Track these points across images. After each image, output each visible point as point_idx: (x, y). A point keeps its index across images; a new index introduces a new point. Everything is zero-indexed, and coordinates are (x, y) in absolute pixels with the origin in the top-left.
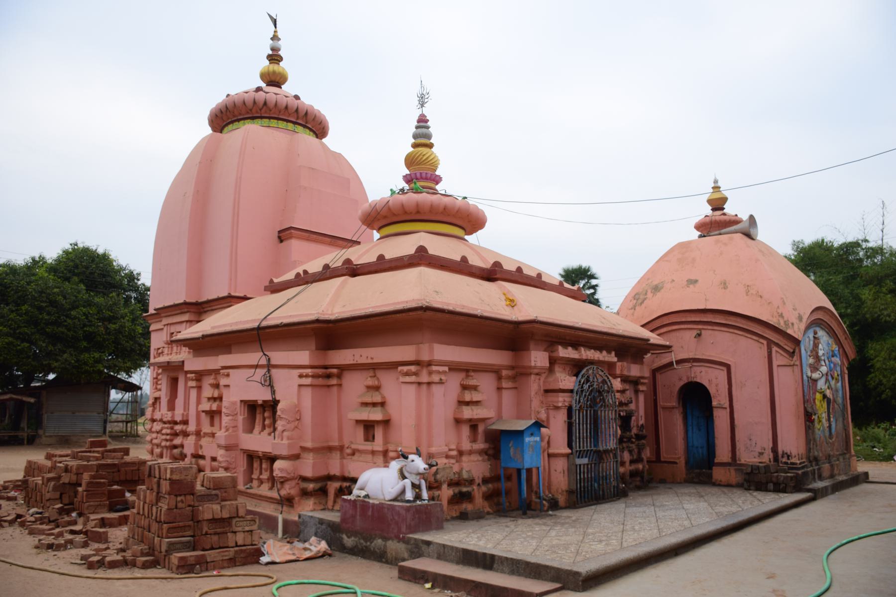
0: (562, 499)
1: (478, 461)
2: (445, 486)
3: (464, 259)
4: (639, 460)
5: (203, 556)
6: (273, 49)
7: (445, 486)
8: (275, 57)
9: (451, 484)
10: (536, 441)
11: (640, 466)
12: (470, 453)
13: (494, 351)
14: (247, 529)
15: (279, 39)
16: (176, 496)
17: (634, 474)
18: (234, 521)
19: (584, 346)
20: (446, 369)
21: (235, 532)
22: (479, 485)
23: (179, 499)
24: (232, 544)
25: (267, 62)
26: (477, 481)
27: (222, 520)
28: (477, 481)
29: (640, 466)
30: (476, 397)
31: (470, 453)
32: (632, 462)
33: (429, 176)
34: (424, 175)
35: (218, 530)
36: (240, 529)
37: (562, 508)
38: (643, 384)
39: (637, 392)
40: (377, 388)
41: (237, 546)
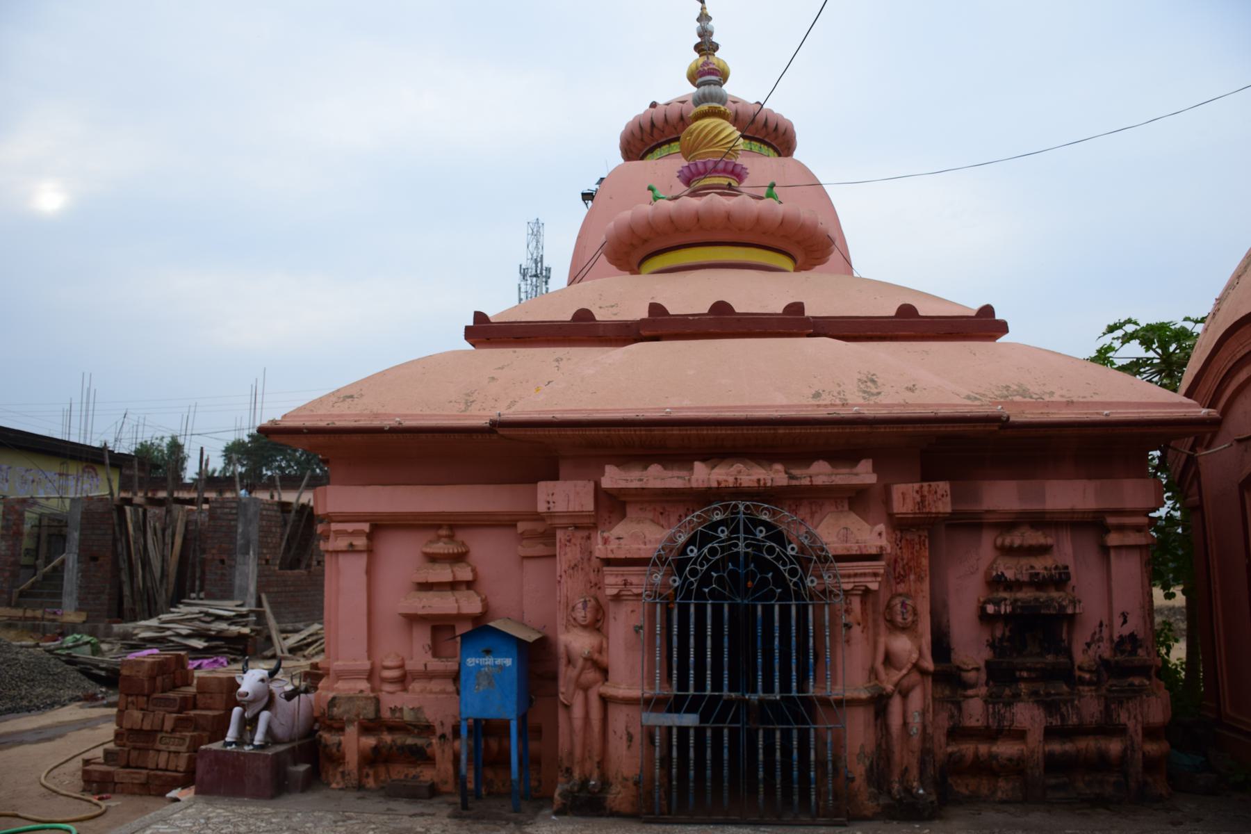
0: (618, 796)
1: (443, 692)
2: (352, 730)
3: (656, 309)
4: (1107, 728)
5: (109, 773)
6: (700, 35)
7: (352, 730)
8: (706, 46)
9: (367, 728)
10: (502, 667)
11: (1115, 747)
12: (428, 675)
13: (492, 487)
14: (172, 748)
15: (710, 19)
16: (128, 695)
17: (1053, 764)
18: (160, 736)
19: (704, 459)
20: (366, 527)
21: (159, 751)
22: (443, 736)
23: (130, 699)
24: (152, 765)
25: (696, 55)
26: (439, 731)
27: (140, 731)
28: (439, 731)
29: (1115, 747)
30: (464, 574)
31: (428, 675)
32: (1050, 733)
33: (710, 166)
34: (700, 166)
35: (140, 745)
36: (163, 747)
37: (614, 814)
38: (1121, 528)
39: (1105, 550)
40: (459, 558)
41: (157, 769)
